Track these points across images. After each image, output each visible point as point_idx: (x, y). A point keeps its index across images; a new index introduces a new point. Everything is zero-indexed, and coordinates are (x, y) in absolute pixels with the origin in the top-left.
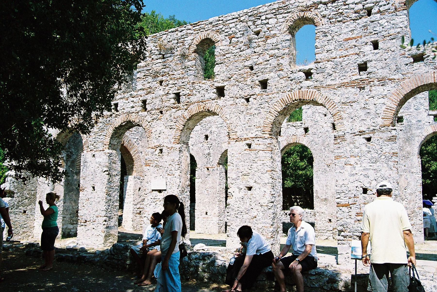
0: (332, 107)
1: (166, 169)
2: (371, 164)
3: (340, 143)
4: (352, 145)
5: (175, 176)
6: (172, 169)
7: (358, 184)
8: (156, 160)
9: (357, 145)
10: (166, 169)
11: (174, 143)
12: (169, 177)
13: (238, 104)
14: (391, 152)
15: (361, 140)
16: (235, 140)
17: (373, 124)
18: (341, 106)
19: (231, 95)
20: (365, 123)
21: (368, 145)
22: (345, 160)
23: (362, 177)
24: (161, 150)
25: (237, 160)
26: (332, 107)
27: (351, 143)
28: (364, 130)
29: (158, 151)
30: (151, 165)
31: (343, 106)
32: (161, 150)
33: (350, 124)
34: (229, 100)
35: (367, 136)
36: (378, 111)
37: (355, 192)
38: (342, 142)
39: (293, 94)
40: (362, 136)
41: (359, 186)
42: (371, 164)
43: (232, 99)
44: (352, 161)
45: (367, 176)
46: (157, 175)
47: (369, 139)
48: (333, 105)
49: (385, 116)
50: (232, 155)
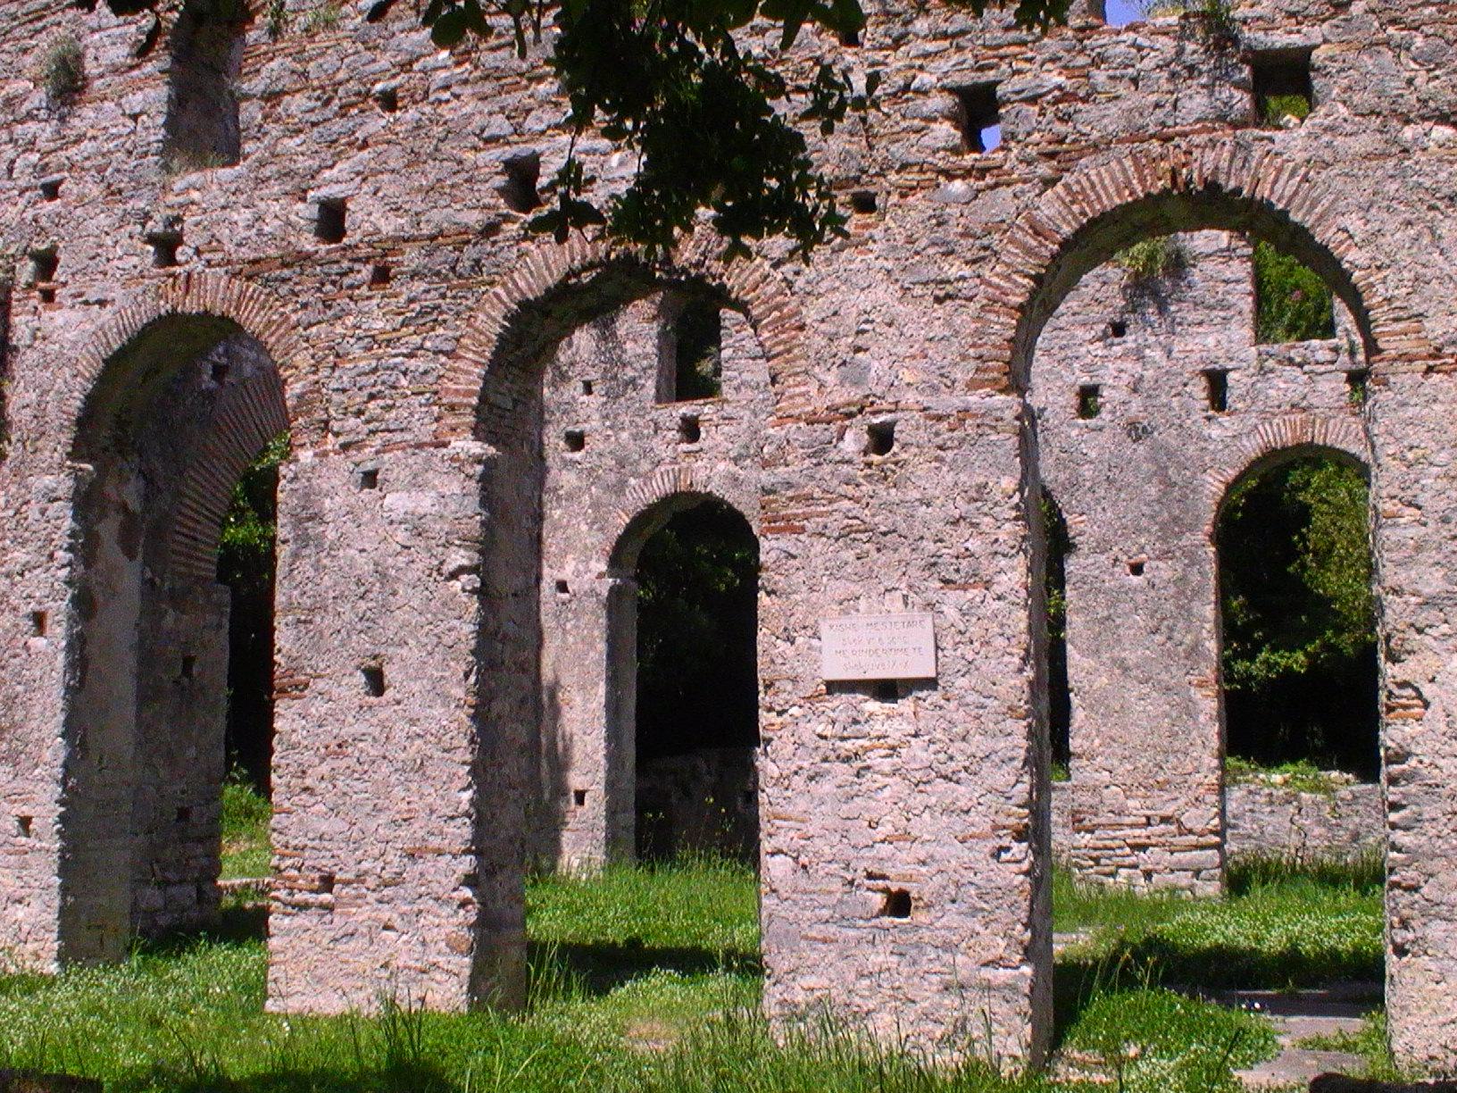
1: (931, 547)
5: (998, 589)
6: (974, 545)
8: (850, 490)
10: (931, 547)
11: (972, 386)
12: (953, 597)
16: (1420, 365)
19: (1363, 99)
24: (882, 439)
25: (1441, 484)
29: (853, 442)
30: (810, 526)
32: (882, 439)
34: (1349, 128)
43: (1376, 122)
46: (856, 589)
50: (1410, 456)
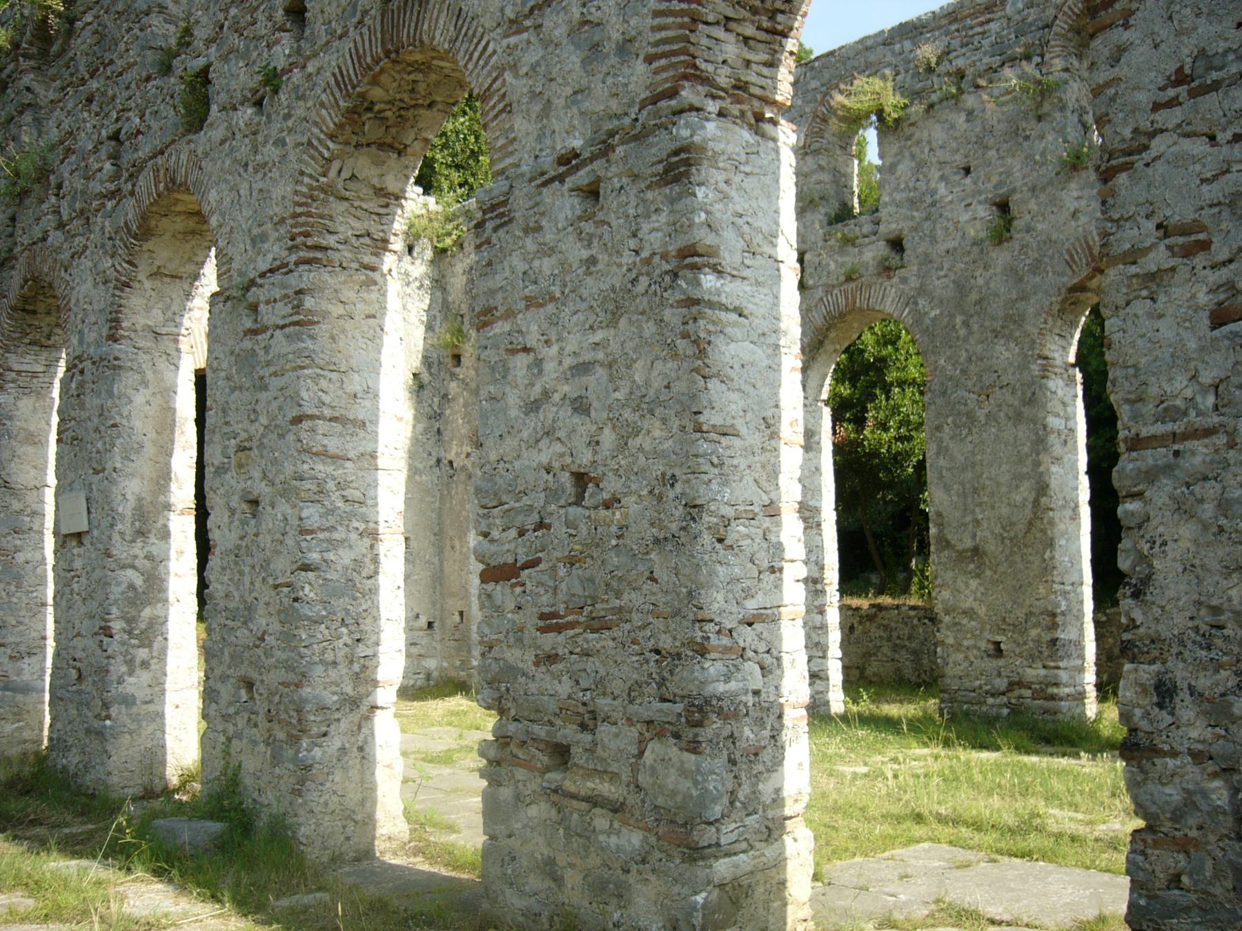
0: (476, 55)
2: (599, 336)
3: (494, 240)
4: (530, 244)
7: (547, 453)
9: (549, 237)
13: (238, 137)
14: (672, 249)
15: (563, 204)
17: (614, 105)
18: (505, 42)
20: (586, 105)
21: (588, 227)
22: (507, 327)
23: (565, 413)
26: (476, 55)
27: (527, 231)
28: (577, 143)
31: (513, 40)
33: (533, 128)
35: (582, 177)
36: (633, 22)
37: (538, 499)
38: (501, 233)
39: (366, 37)
40: (570, 181)
41: (556, 465)
42: (599, 336)
44: (532, 327)
45: (580, 406)
47: (592, 193)
48: (480, 48)
49: (656, 44)
